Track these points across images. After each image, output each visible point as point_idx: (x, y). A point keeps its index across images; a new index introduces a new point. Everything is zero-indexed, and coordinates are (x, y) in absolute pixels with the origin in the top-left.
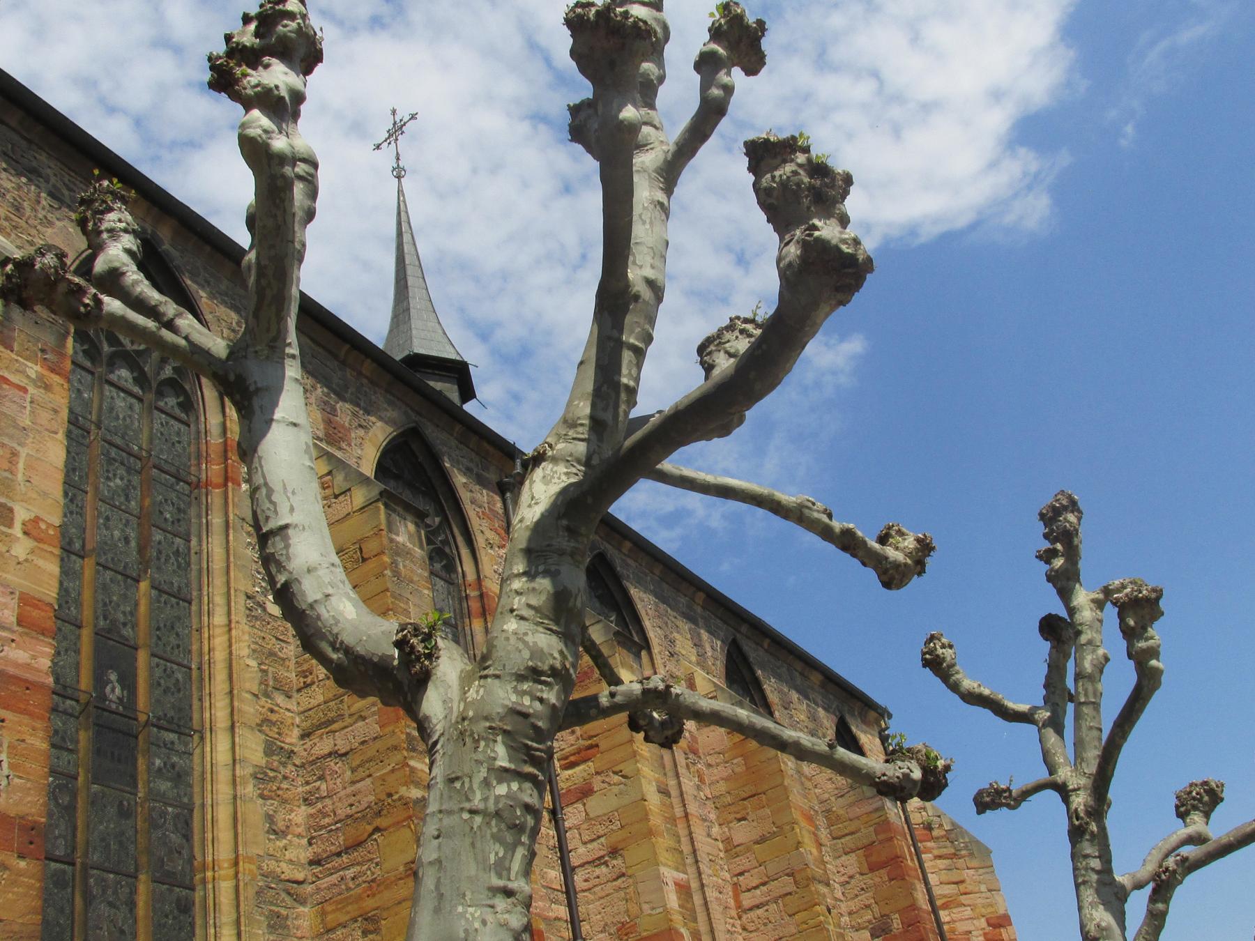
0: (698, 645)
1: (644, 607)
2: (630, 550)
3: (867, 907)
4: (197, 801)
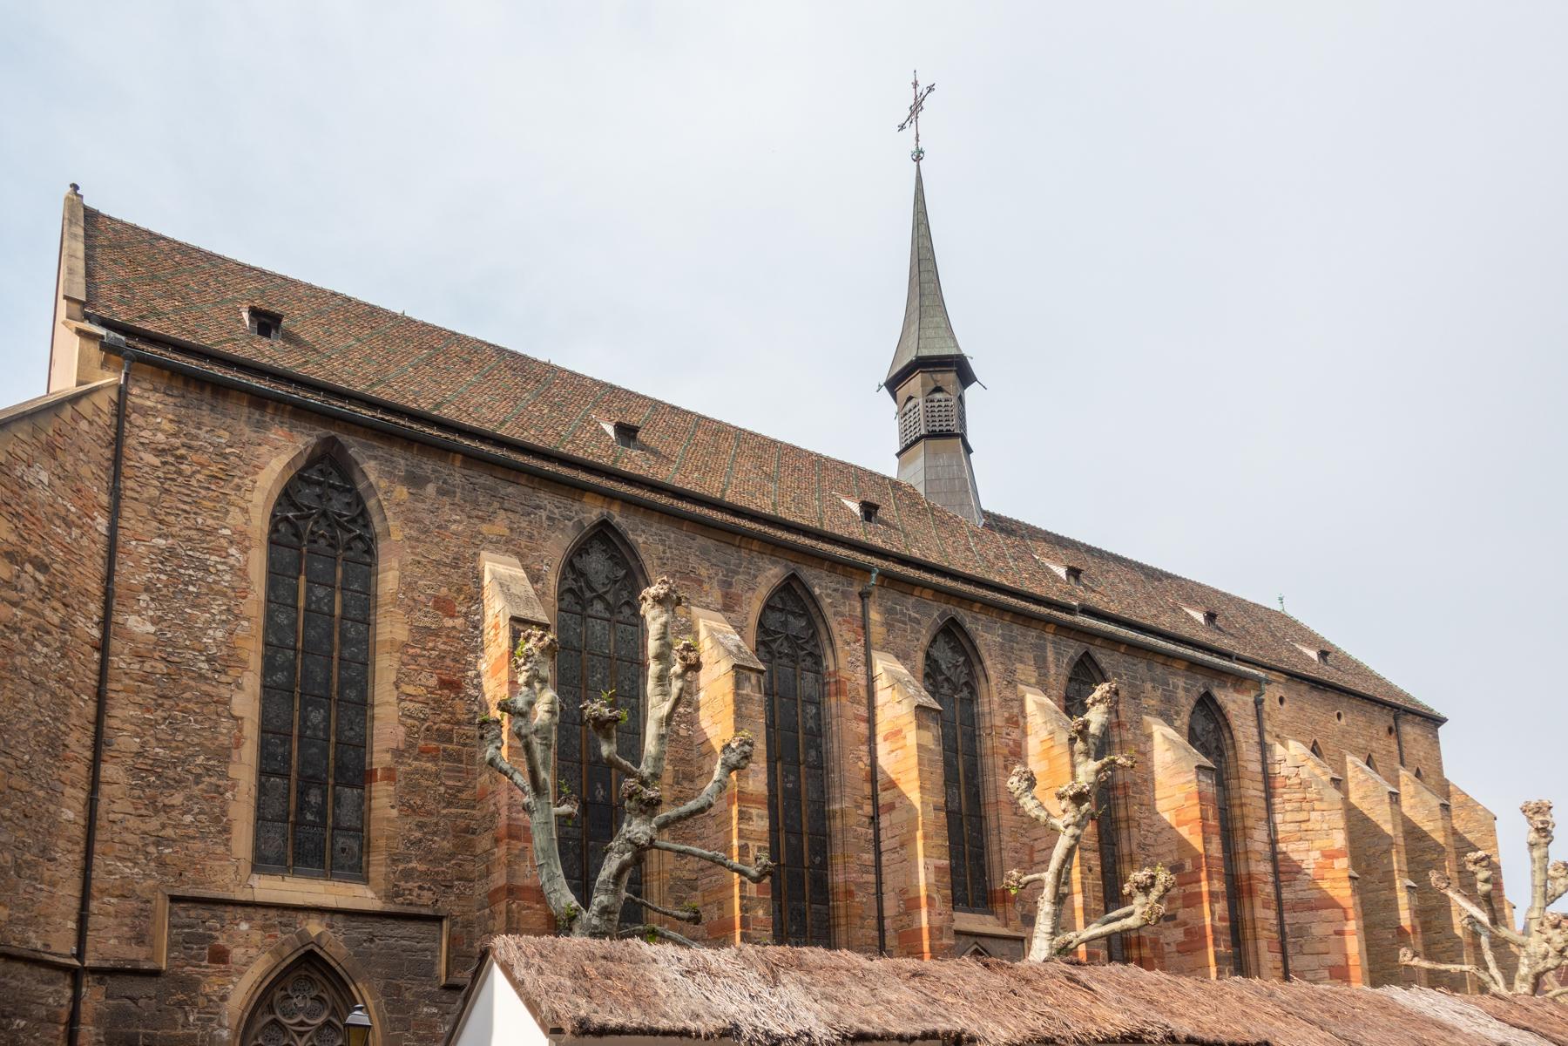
0: (1041, 664)
3: (1171, 851)
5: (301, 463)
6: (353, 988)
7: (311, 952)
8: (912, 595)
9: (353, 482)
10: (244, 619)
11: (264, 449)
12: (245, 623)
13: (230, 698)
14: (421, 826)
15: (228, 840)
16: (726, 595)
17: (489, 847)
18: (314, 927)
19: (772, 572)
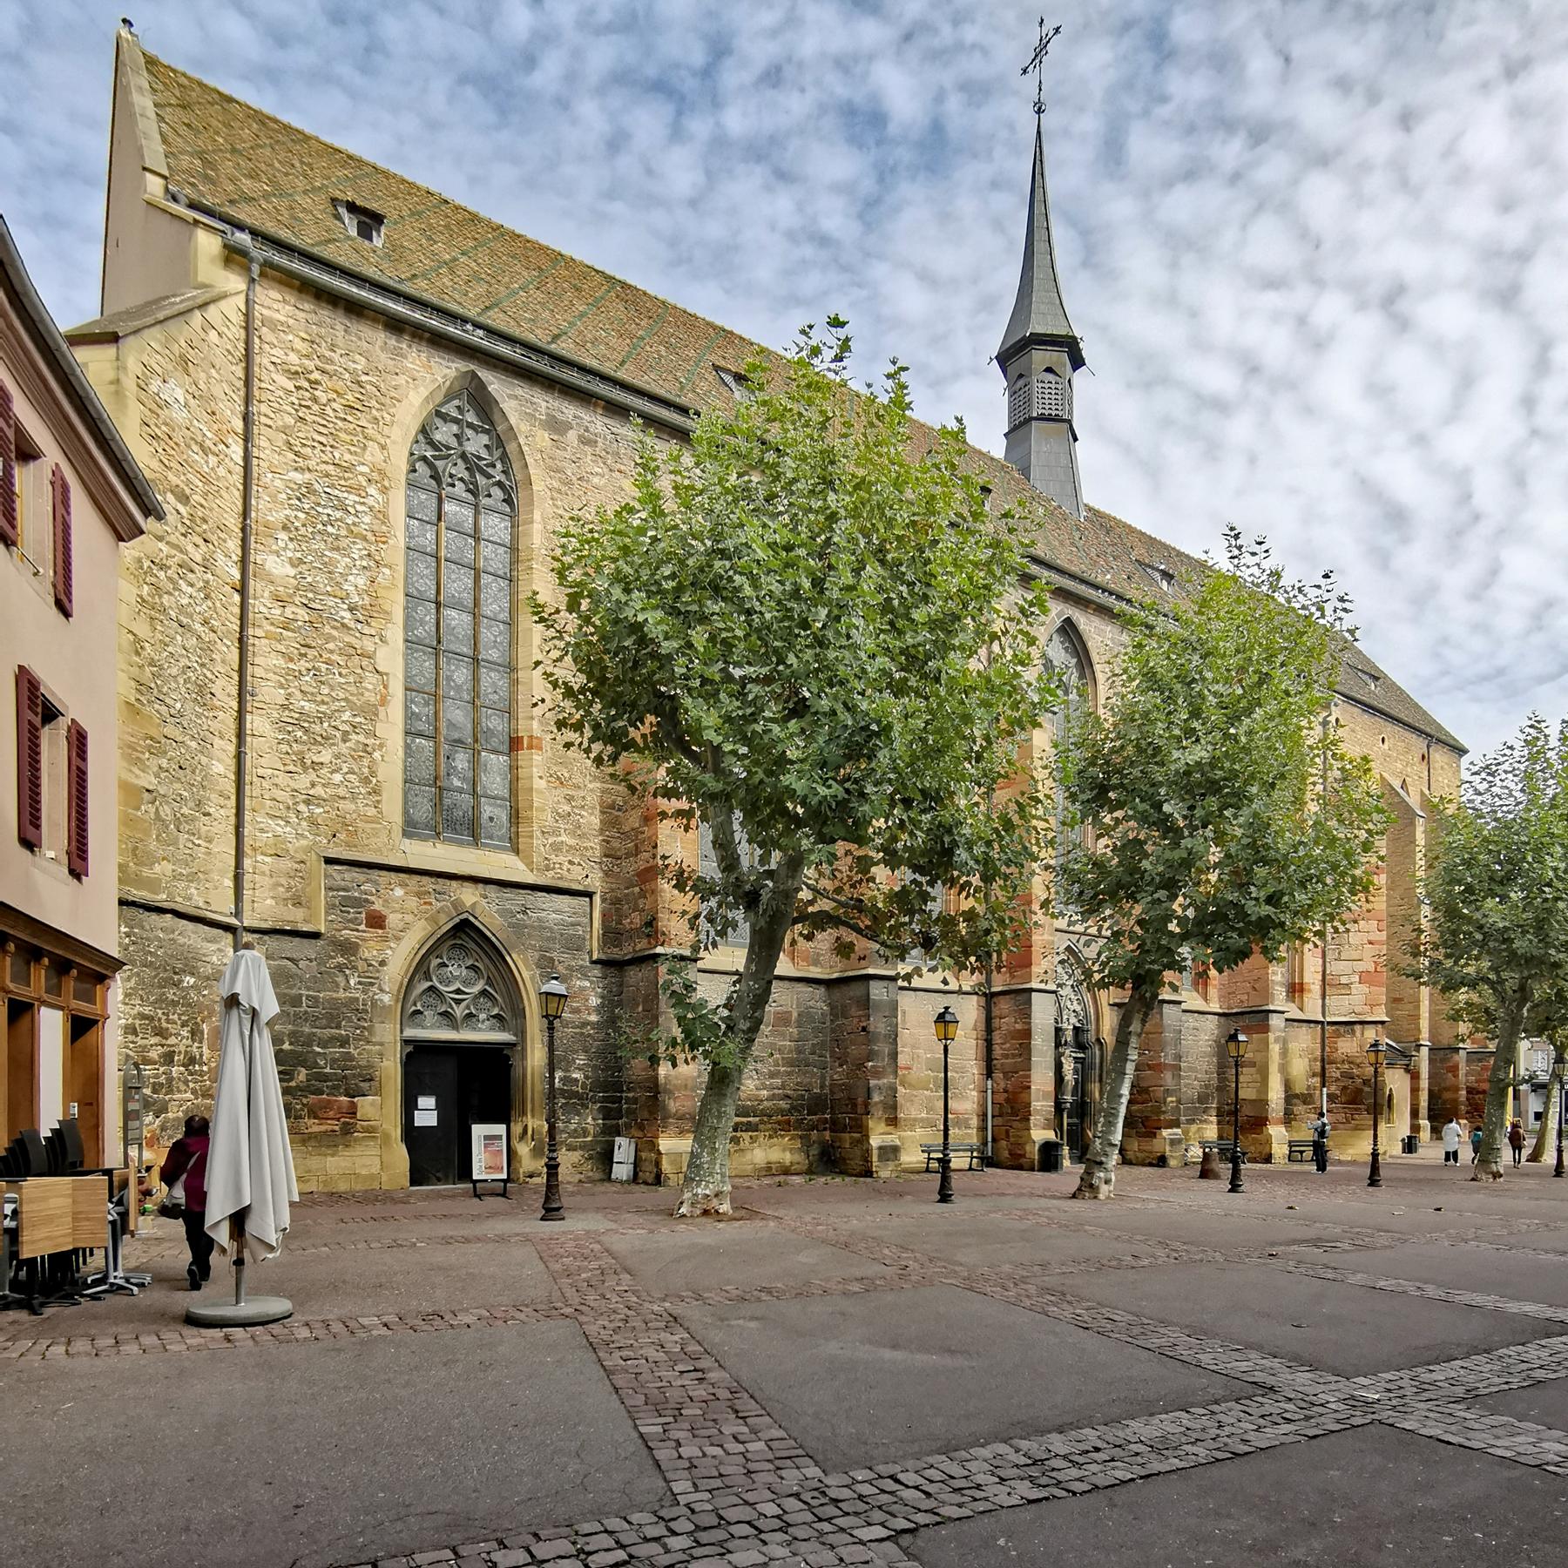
5: (439, 398)
6: (508, 958)
7: (466, 920)
9: (492, 423)
10: (385, 566)
11: (401, 380)
12: (387, 571)
13: (375, 652)
14: (569, 799)
15: (378, 802)
17: (637, 825)
18: (469, 896)
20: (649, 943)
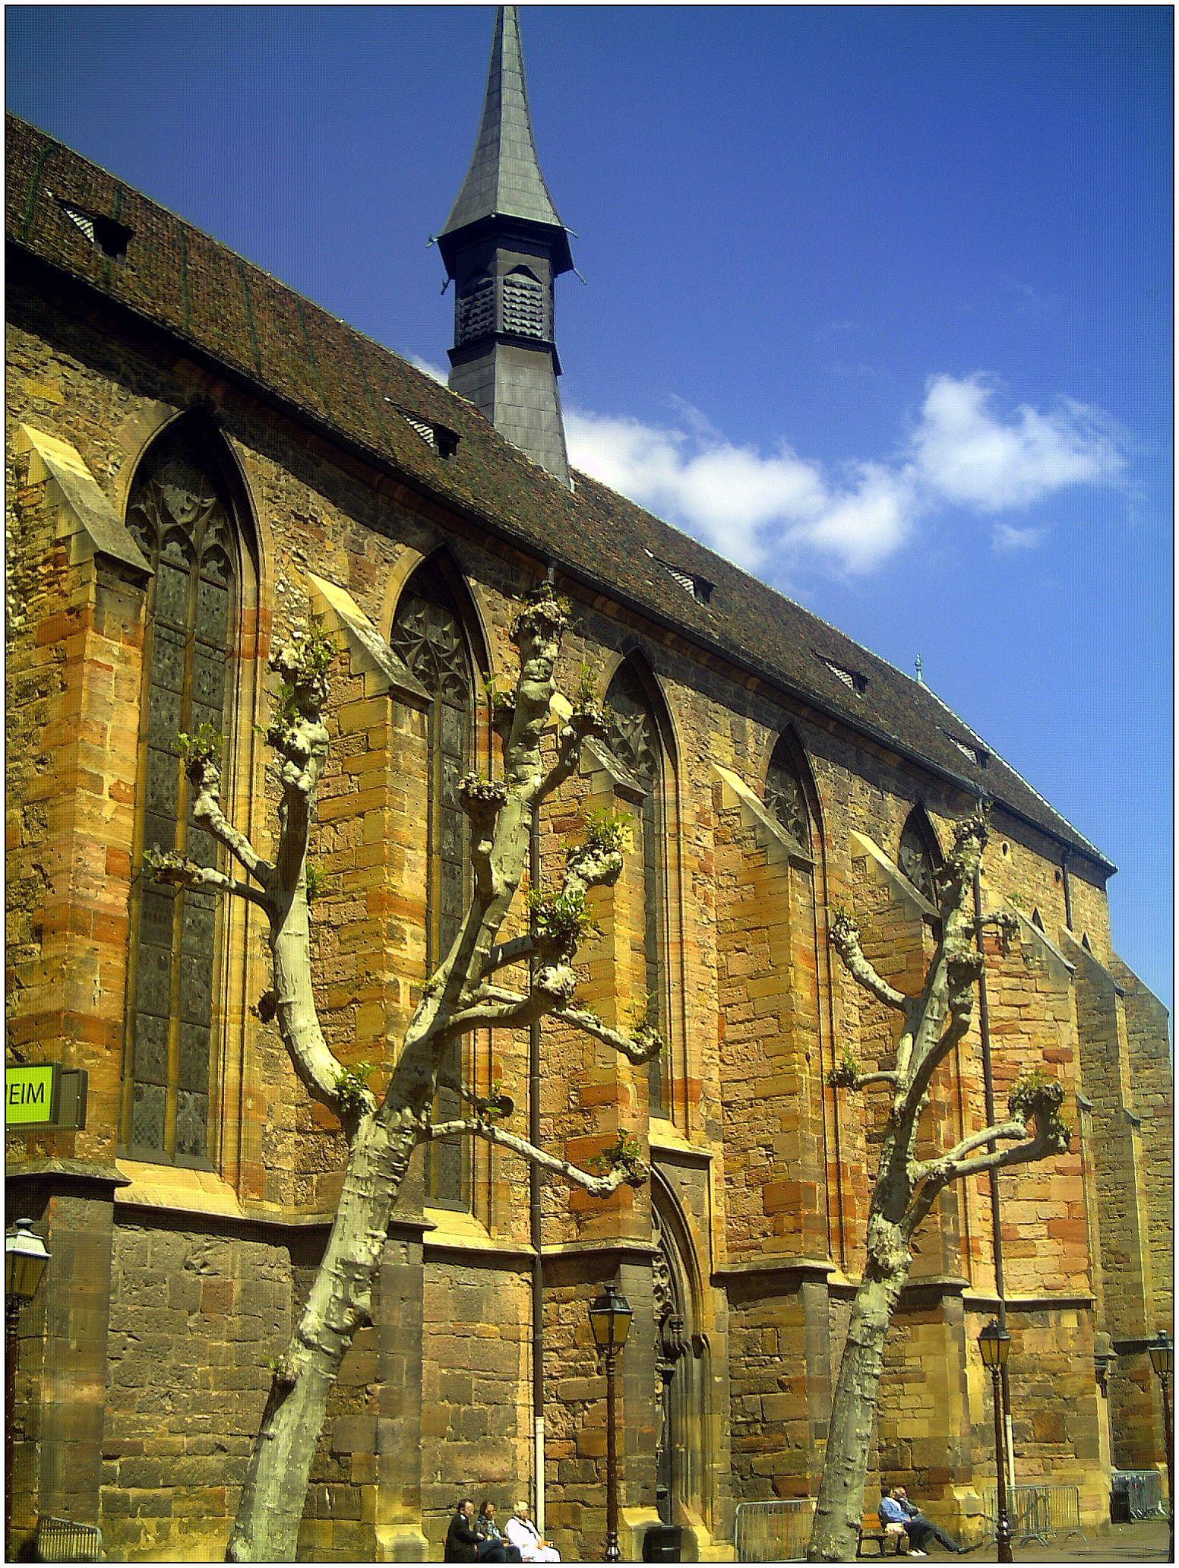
1: (679, 706)
2: (673, 641)
4: (216, 953)
8: (591, 606)
16: (355, 564)
19: (417, 538)
20: (30, 1151)
